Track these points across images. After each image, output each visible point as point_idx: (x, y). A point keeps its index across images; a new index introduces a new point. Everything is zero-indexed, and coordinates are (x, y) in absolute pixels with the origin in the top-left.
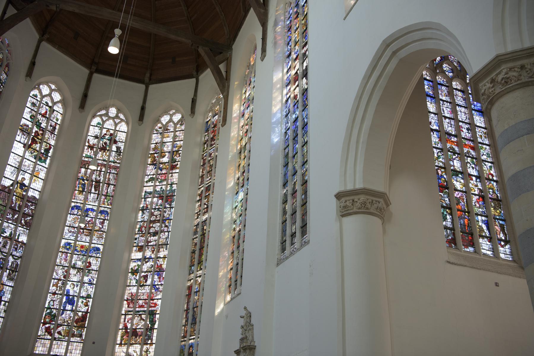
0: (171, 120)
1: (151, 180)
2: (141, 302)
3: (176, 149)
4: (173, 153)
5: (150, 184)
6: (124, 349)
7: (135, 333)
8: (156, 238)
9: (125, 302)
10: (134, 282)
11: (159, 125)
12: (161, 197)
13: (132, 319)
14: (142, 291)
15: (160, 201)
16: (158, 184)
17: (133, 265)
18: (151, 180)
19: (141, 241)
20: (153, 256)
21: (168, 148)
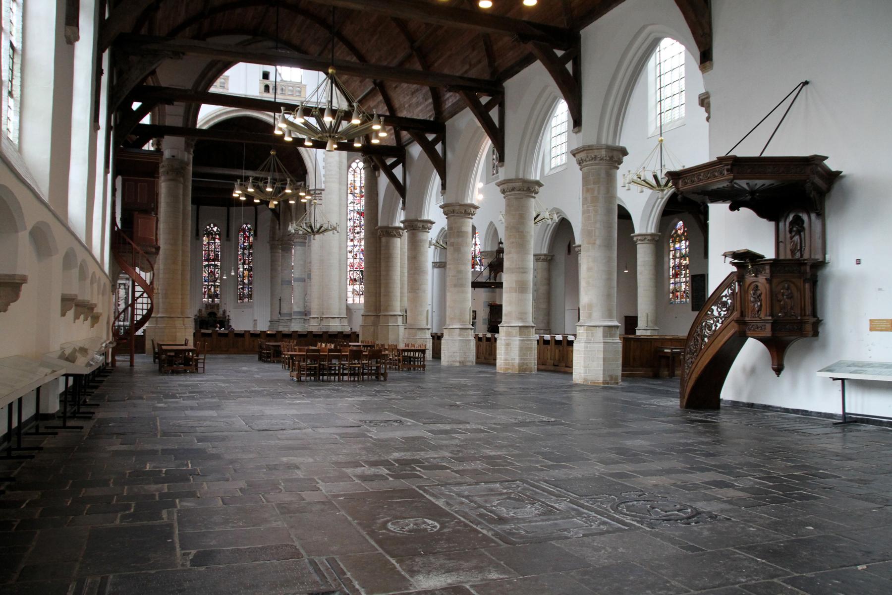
0: (357, 167)
1: (352, 202)
2: (356, 266)
3: (362, 185)
4: (361, 187)
5: (352, 205)
6: (352, 286)
7: (355, 280)
8: (359, 235)
9: (348, 267)
10: (351, 257)
11: (351, 169)
12: (358, 213)
13: (353, 274)
14: (355, 261)
15: (358, 216)
16: (355, 205)
17: (349, 249)
18: (352, 202)
19: (351, 236)
20: (358, 244)
21: (358, 184)
